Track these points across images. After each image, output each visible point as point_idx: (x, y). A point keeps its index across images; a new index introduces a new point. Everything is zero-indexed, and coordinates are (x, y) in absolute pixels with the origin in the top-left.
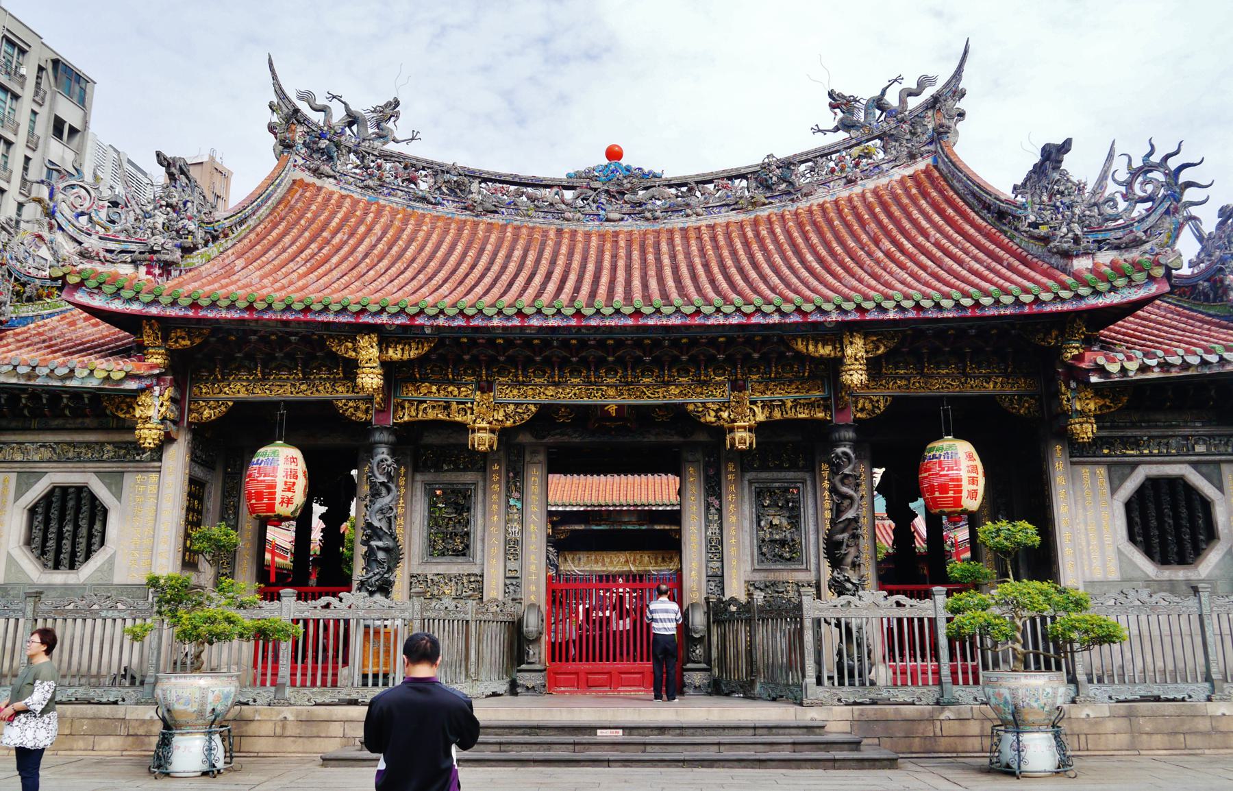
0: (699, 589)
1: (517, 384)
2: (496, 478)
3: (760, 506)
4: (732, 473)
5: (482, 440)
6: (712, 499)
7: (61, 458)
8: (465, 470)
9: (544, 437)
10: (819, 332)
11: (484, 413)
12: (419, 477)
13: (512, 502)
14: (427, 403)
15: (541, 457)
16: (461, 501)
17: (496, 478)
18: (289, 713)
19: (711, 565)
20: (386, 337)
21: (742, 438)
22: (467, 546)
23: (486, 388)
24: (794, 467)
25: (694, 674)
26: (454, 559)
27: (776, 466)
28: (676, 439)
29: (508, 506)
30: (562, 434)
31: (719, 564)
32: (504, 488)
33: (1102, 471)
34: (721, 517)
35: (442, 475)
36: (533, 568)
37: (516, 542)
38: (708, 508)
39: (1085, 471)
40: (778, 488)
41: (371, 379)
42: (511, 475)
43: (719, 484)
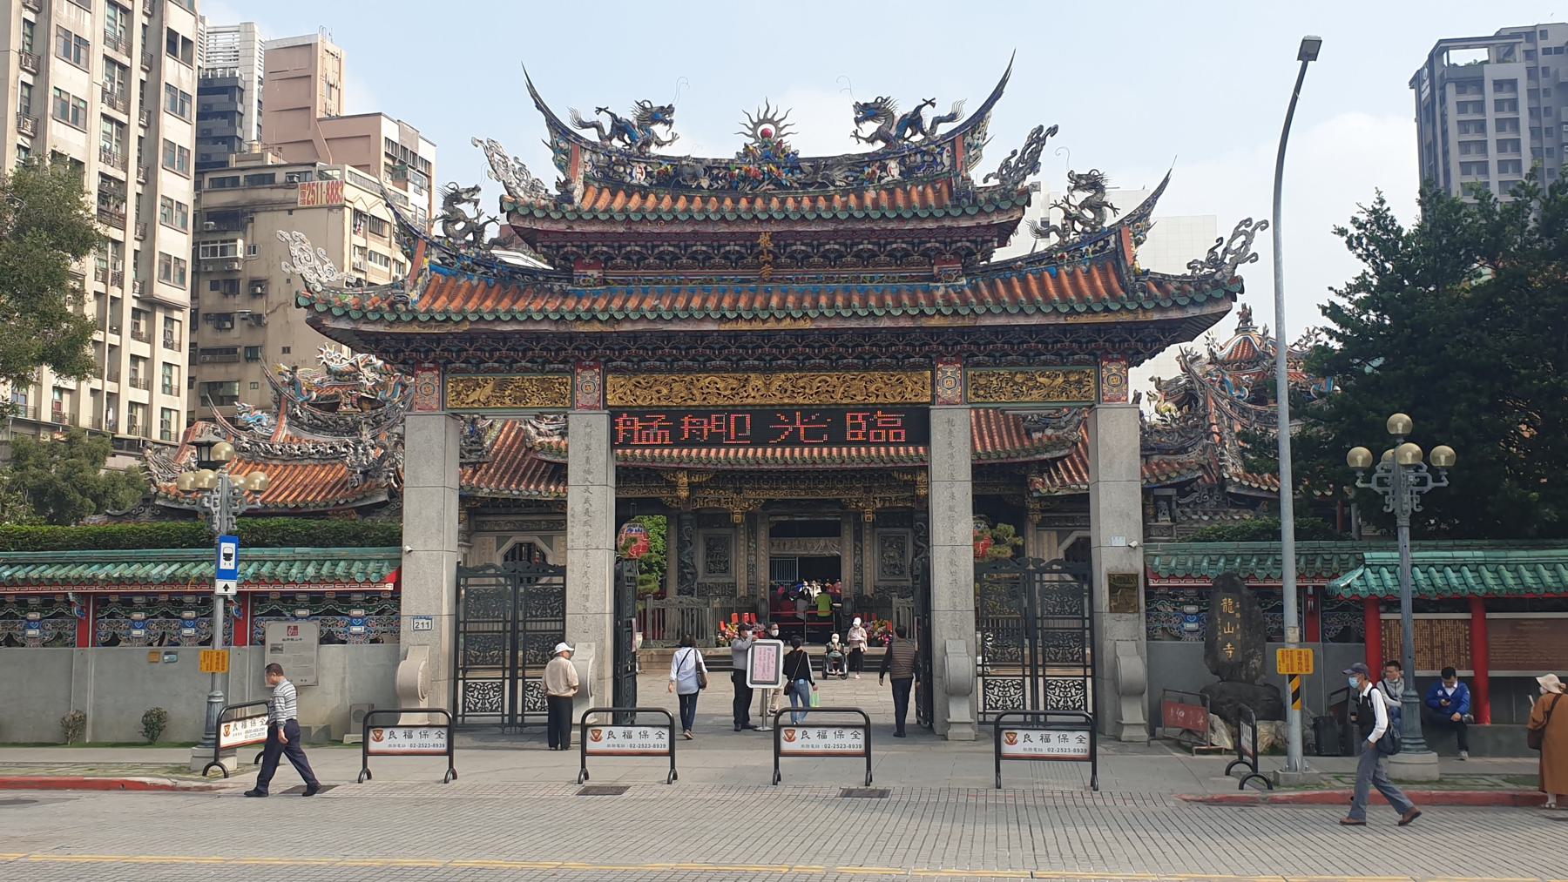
1: (753, 489)
3: (883, 545)
5: (737, 518)
7: (522, 528)
10: (906, 470)
11: (738, 506)
12: (701, 531)
14: (711, 498)
18: (653, 651)
20: (691, 472)
21: (869, 517)
23: (739, 491)
24: (902, 526)
33: (1054, 534)
39: (1045, 535)
41: (684, 494)
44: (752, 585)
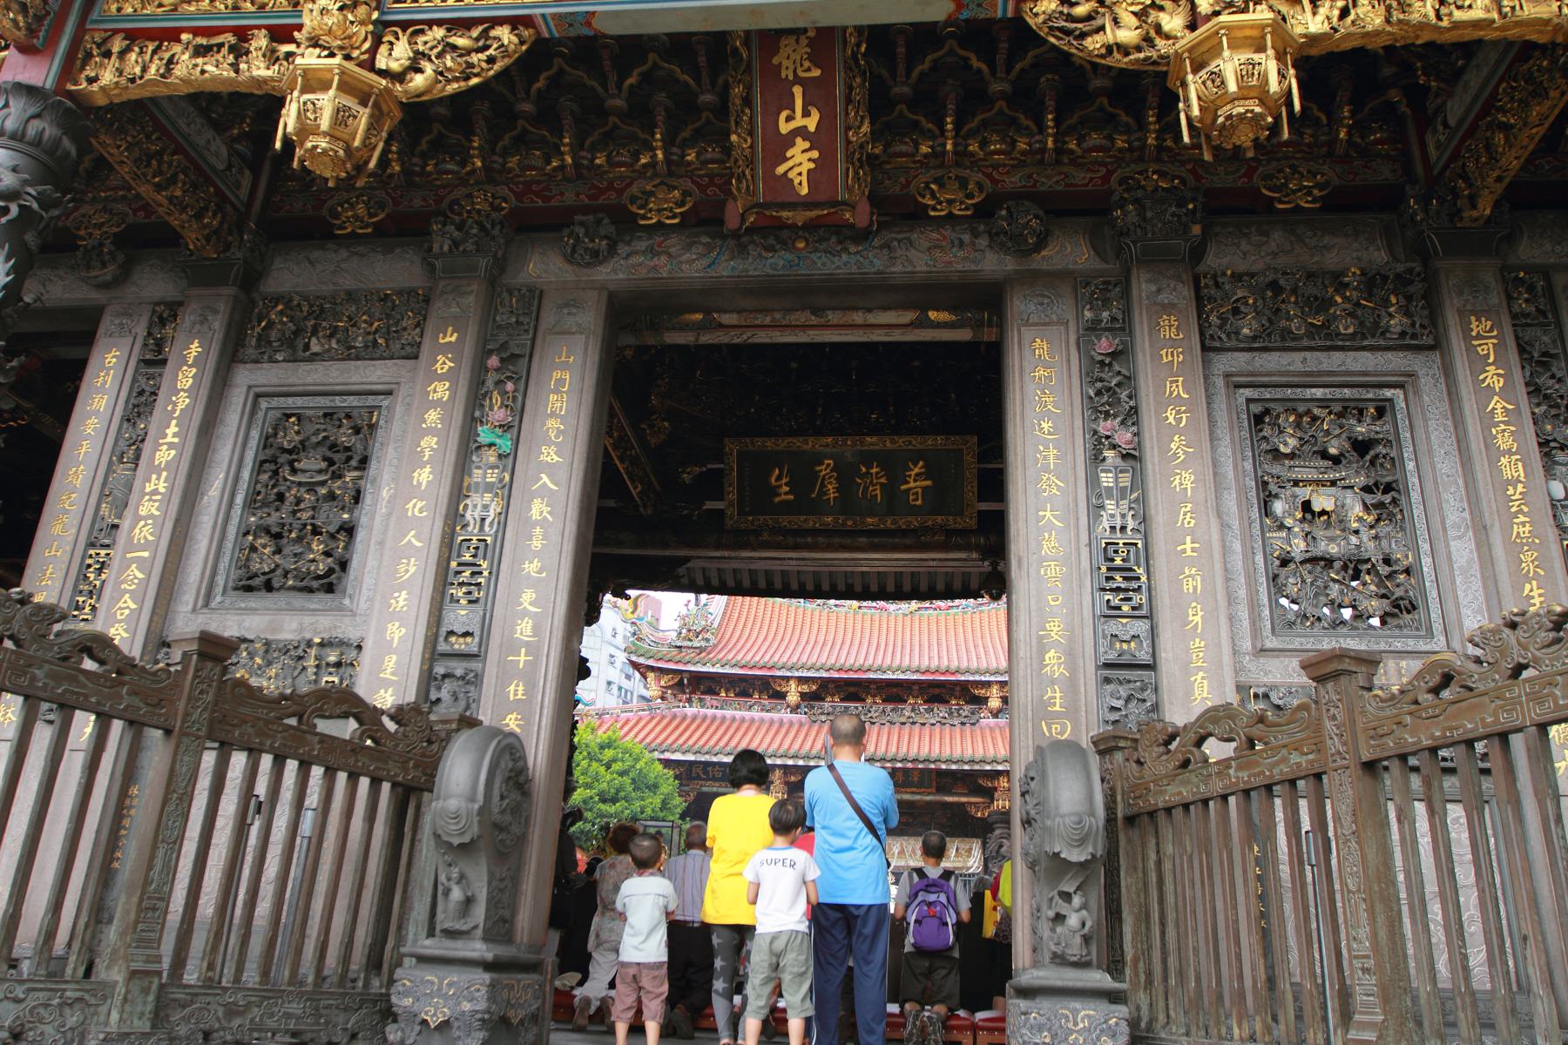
0: (1071, 712)
2: (443, 364)
4: (1173, 344)
6: (1104, 427)
8: (371, 352)
9: (596, 258)
13: (485, 434)
15: (590, 318)
16: (345, 437)
17: (443, 364)
19: (1114, 627)
22: (344, 565)
24: (1368, 335)
25: (1064, 1007)
26: (299, 600)
27: (1313, 331)
28: (993, 264)
29: (468, 448)
30: (652, 252)
31: (1141, 627)
32: (462, 392)
34: (1139, 481)
35: (304, 367)
36: (524, 629)
37: (482, 548)
38: (1096, 458)
40: (1324, 403)
42: (493, 361)
43: (1129, 380)
44: (448, 661)
